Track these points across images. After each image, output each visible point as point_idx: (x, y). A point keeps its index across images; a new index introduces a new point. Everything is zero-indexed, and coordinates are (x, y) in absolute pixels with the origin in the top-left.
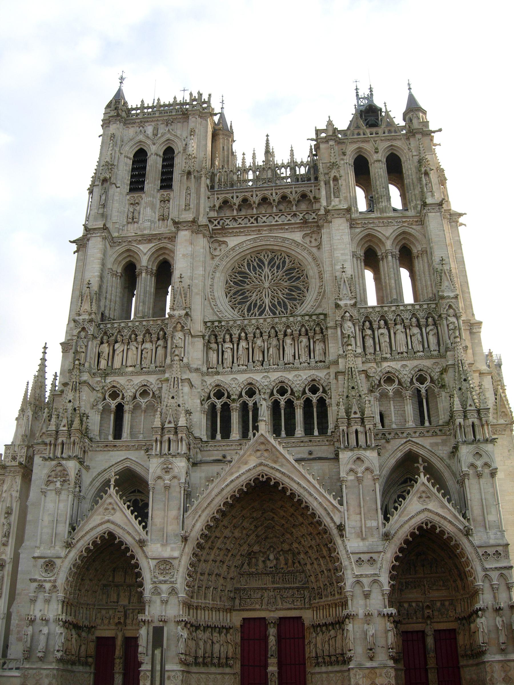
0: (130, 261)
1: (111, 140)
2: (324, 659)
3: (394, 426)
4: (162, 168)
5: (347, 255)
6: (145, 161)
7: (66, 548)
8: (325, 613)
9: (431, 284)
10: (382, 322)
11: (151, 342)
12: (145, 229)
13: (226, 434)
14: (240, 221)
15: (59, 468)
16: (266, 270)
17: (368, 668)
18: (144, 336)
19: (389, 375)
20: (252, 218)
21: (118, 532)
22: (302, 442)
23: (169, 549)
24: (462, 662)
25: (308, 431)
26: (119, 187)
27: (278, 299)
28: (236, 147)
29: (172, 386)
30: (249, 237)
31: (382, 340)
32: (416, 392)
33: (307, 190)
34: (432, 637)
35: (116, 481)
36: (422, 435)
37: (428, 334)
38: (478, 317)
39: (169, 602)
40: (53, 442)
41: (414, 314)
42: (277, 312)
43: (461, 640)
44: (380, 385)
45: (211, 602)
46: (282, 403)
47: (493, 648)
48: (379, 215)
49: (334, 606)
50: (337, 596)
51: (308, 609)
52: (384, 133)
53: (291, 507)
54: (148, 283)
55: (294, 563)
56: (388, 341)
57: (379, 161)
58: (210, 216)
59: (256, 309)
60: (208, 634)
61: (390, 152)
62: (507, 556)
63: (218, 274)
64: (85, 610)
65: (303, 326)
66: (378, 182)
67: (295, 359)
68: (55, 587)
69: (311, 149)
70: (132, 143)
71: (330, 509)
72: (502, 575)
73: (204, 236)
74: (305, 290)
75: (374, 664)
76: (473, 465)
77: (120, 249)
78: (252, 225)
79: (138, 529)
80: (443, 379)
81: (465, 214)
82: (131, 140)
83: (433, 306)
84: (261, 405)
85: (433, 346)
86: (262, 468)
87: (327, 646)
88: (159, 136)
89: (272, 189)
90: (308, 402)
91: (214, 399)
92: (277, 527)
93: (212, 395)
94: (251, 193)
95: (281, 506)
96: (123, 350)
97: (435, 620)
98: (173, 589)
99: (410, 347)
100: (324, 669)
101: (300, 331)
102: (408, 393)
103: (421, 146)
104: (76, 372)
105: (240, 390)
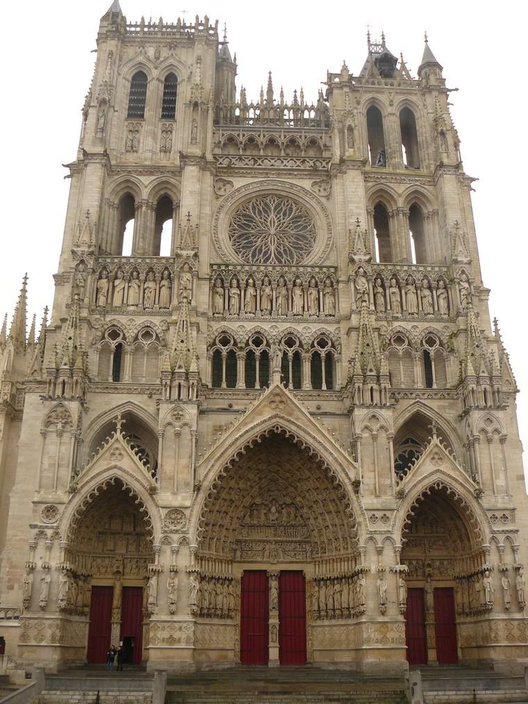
0: (128, 192)
1: (109, 58)
2: (327, 612)
3: (403, 386)
4: (164, 96)
5: (362, 209)
6: (145, 86)
7: (69, 493)
8: (328, 568)
9: (441, 247)
10: (394, 281)
11: (154, 281)
12: (146, 159)
13: (232, 382)
14: (247, 160)
15: (60, 409)
16: (272, 215)
17: (380, 622)
18: (147, 275)
19: (399, 335)
20: (259, 159)
21: (126, 478)
22: (311, 395)
23: (179, 498)
24: (459, 620)
25: (316, 384)
26: (117, 111)
27: (284, 247)
28: (239, 81)
29: (181, 330)
30: (256, 180)
31: (394, 299)
32: (424, 353)
33: (317, 136)
34: (432, 594)
35: (123, 425)
36: (430, 398)
37: (438, 297)
38: (486, 285)
39: (180, 552)
40: (53, 380)
41: (425, 276)
42: (283, 261)
43: (459, 598)
44: (390, 344)
45: (215, 553)
46: (290, 354)
47: (497, 608)
48: (391, 170)
49: (339, 561)
50: (342, 552)
51: (310, 563)
52: (399, 86)
53: (299, 461)
54: (149, 218)
55: (296, 517)
56: (399, 300)
57: (394, 114)
58: (214, 152)
59: (261, 255)
60: (212, 585)
61: (404, 106)
62: (513, 520)
63: (222, 216)
64: (81, 557)
65: (313, 277)
66: (391, 136)
67: (304, 311)
68: (57, 533)
69: (321, 94)
70: (132, 64)
71: (345, 464)
72: (508, 538)
73: (212, 174)
74: (313, 240)
75: (386, 619)
76: (483, 430)
77: (118, 178)
78: (259, 167)
79: (147, 476)
80: (451, 344)
81: (478, 179)
82: (130, 60)
83: (445, 269)
84: (278, 355)
85: (443, 310)
86: (278, 419)
87: (331, 600)
88: (162, 59)
89: (281, 132)
90: (316, 356)
91: (219, 346)
92: (281, 481)
93: (217, 342)
94: (258, 133)
95: (288, 460)
96: (124, 288)
97: (434, 578)
98: (184, 539)
99: (421, 309)
100: (326, 622)
101: (309, 282)
102: (419, 354)
103: (437, 104)
104: (74, 307)
105: (247, 338)
